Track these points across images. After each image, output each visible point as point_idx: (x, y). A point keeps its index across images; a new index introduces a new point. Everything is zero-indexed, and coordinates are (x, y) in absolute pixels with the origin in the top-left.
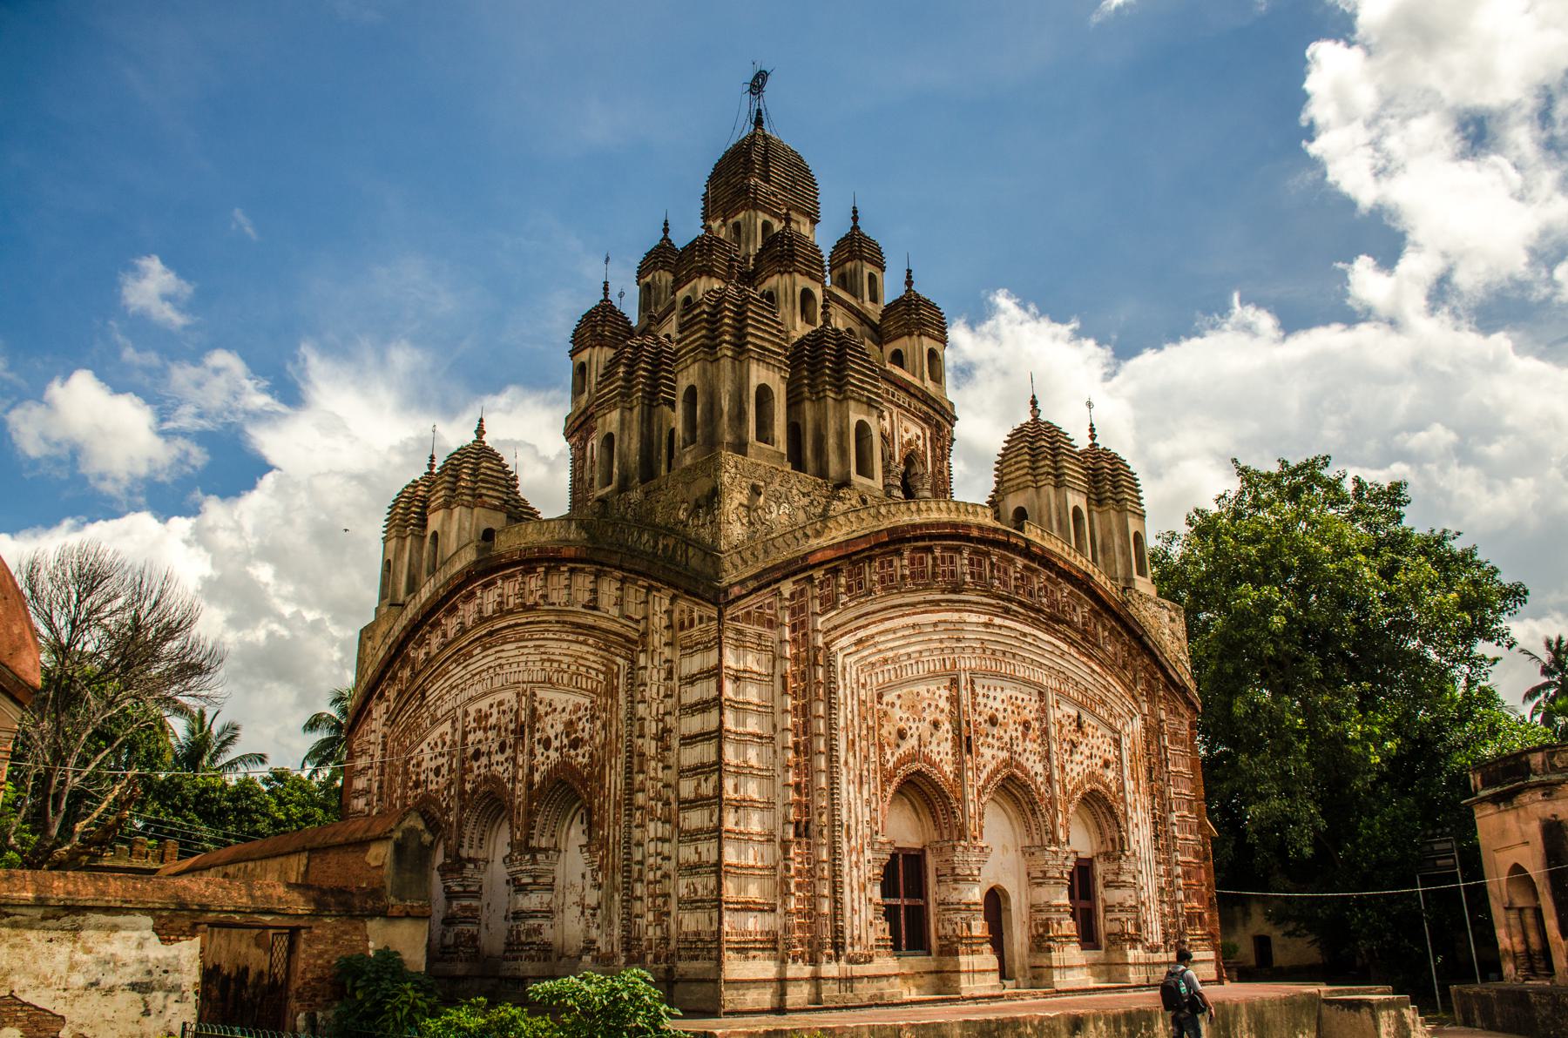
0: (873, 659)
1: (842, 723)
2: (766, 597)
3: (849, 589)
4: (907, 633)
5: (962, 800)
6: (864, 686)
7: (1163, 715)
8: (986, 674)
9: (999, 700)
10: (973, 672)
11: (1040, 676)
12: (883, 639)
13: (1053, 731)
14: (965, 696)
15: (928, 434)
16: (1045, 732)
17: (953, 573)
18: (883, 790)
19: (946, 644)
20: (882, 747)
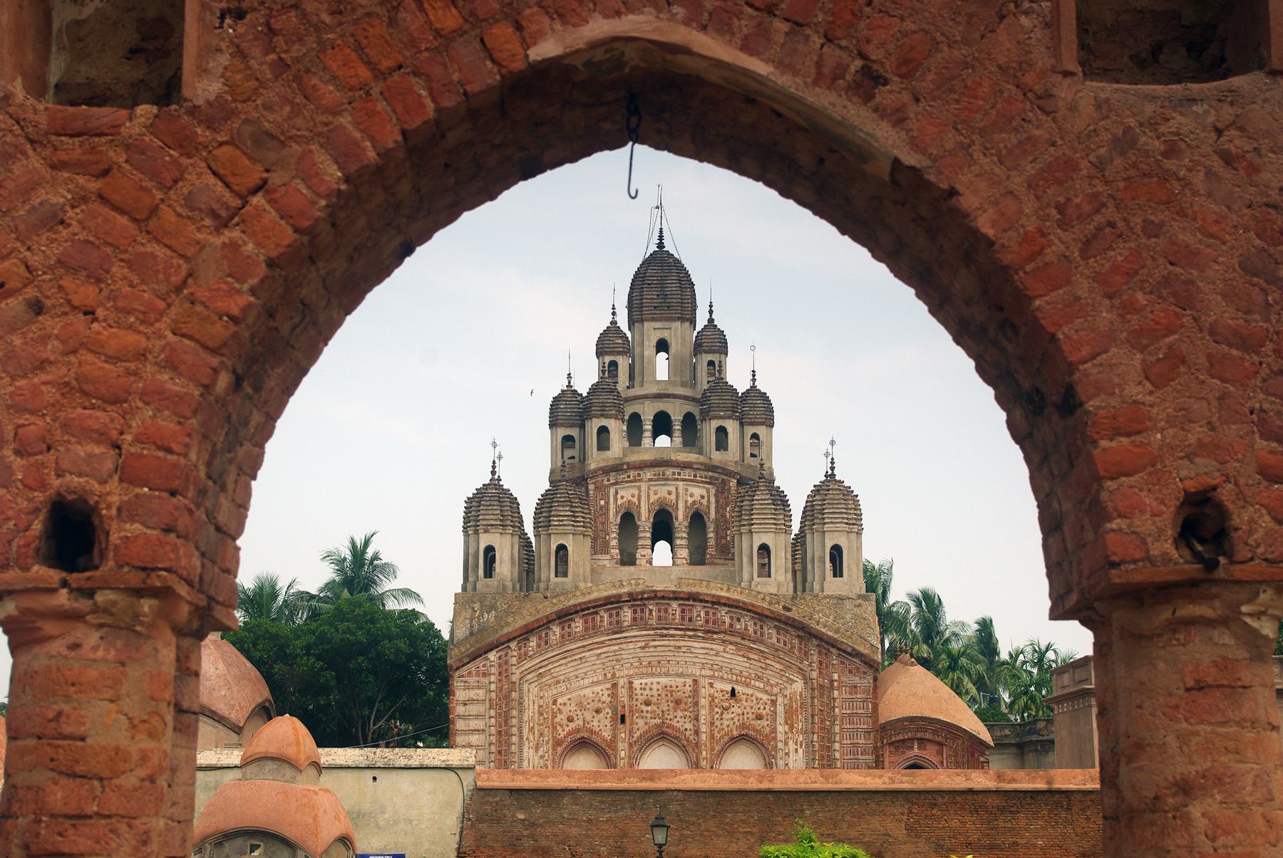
0: (548, 683)
1: (526, 718)
2: (479, 662)
3: (539, 646)
4: (575, 663)
5: (615, 749)
6: (541, 698)
7: (836, 676)
8: (642, 675)
9: (655, 690)
10: (629, 676)
11: (696, 671)
12: (557, 670)
13: (703, 702)
14: (623, 693)
15: (713, 491)
16: (696, 704)
17: (618, 622)
18: (554, 749)
19: (609, 664)
20: (554, 728)
